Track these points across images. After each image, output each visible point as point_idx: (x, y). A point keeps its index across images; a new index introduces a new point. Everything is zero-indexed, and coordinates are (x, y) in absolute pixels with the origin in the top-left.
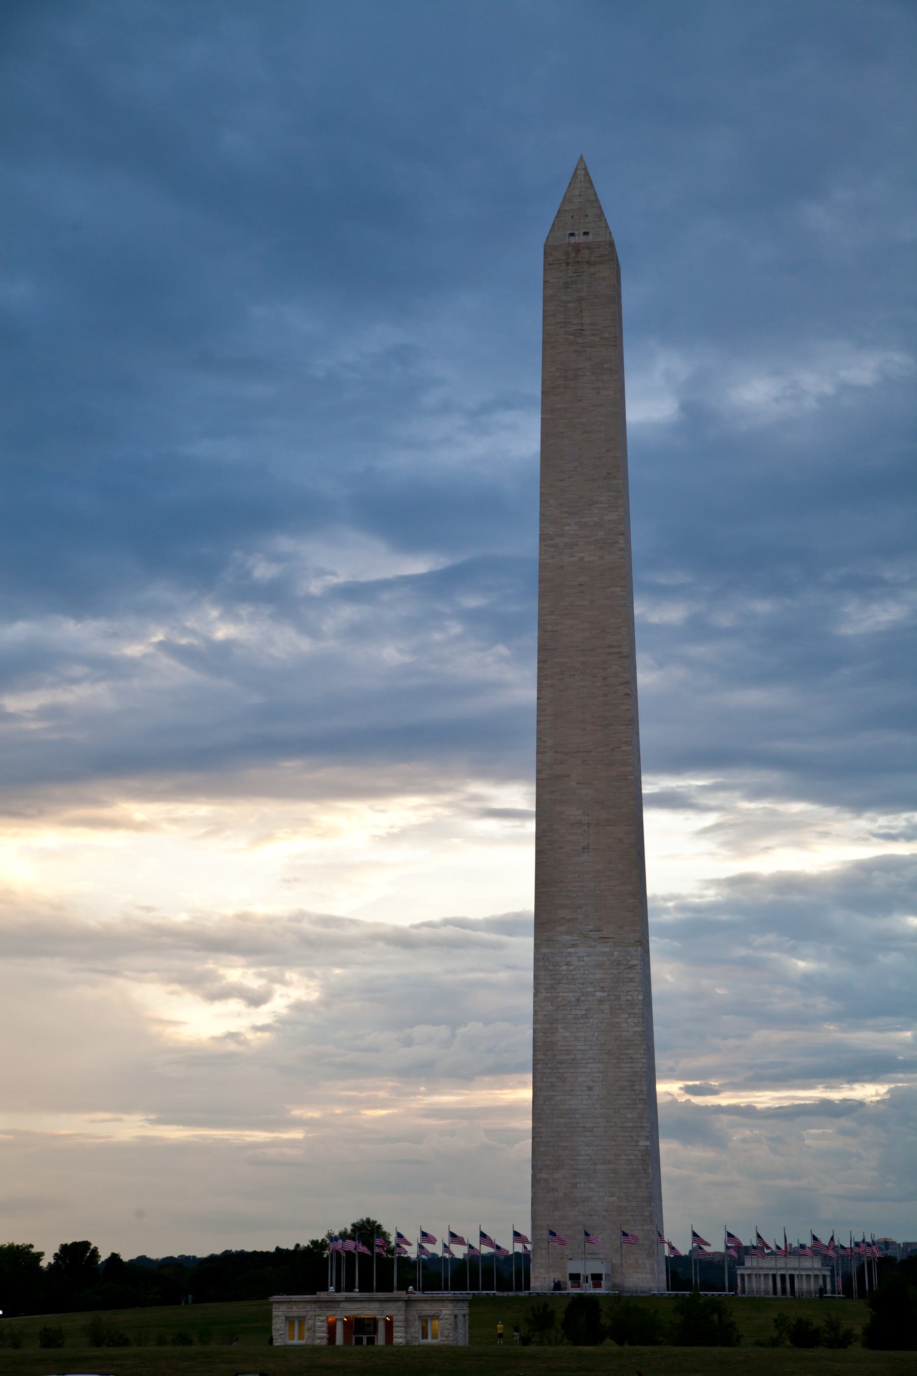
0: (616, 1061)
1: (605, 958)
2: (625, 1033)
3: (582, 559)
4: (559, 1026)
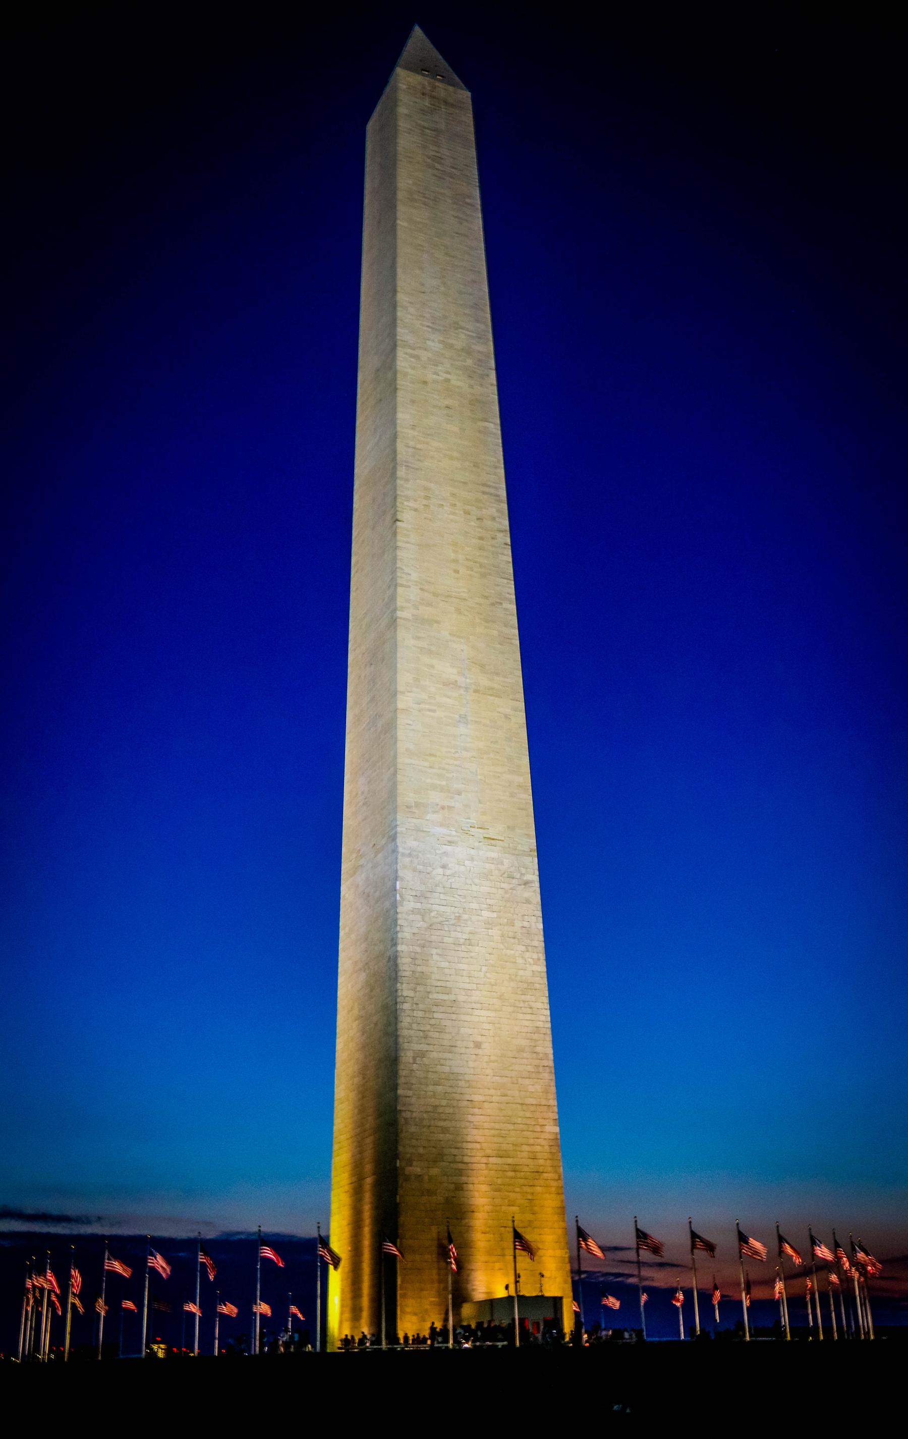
0: (510, 1009)
1: (493, 867)
2: (521, 973)
3: (447, 381)
4: (434, 951)
